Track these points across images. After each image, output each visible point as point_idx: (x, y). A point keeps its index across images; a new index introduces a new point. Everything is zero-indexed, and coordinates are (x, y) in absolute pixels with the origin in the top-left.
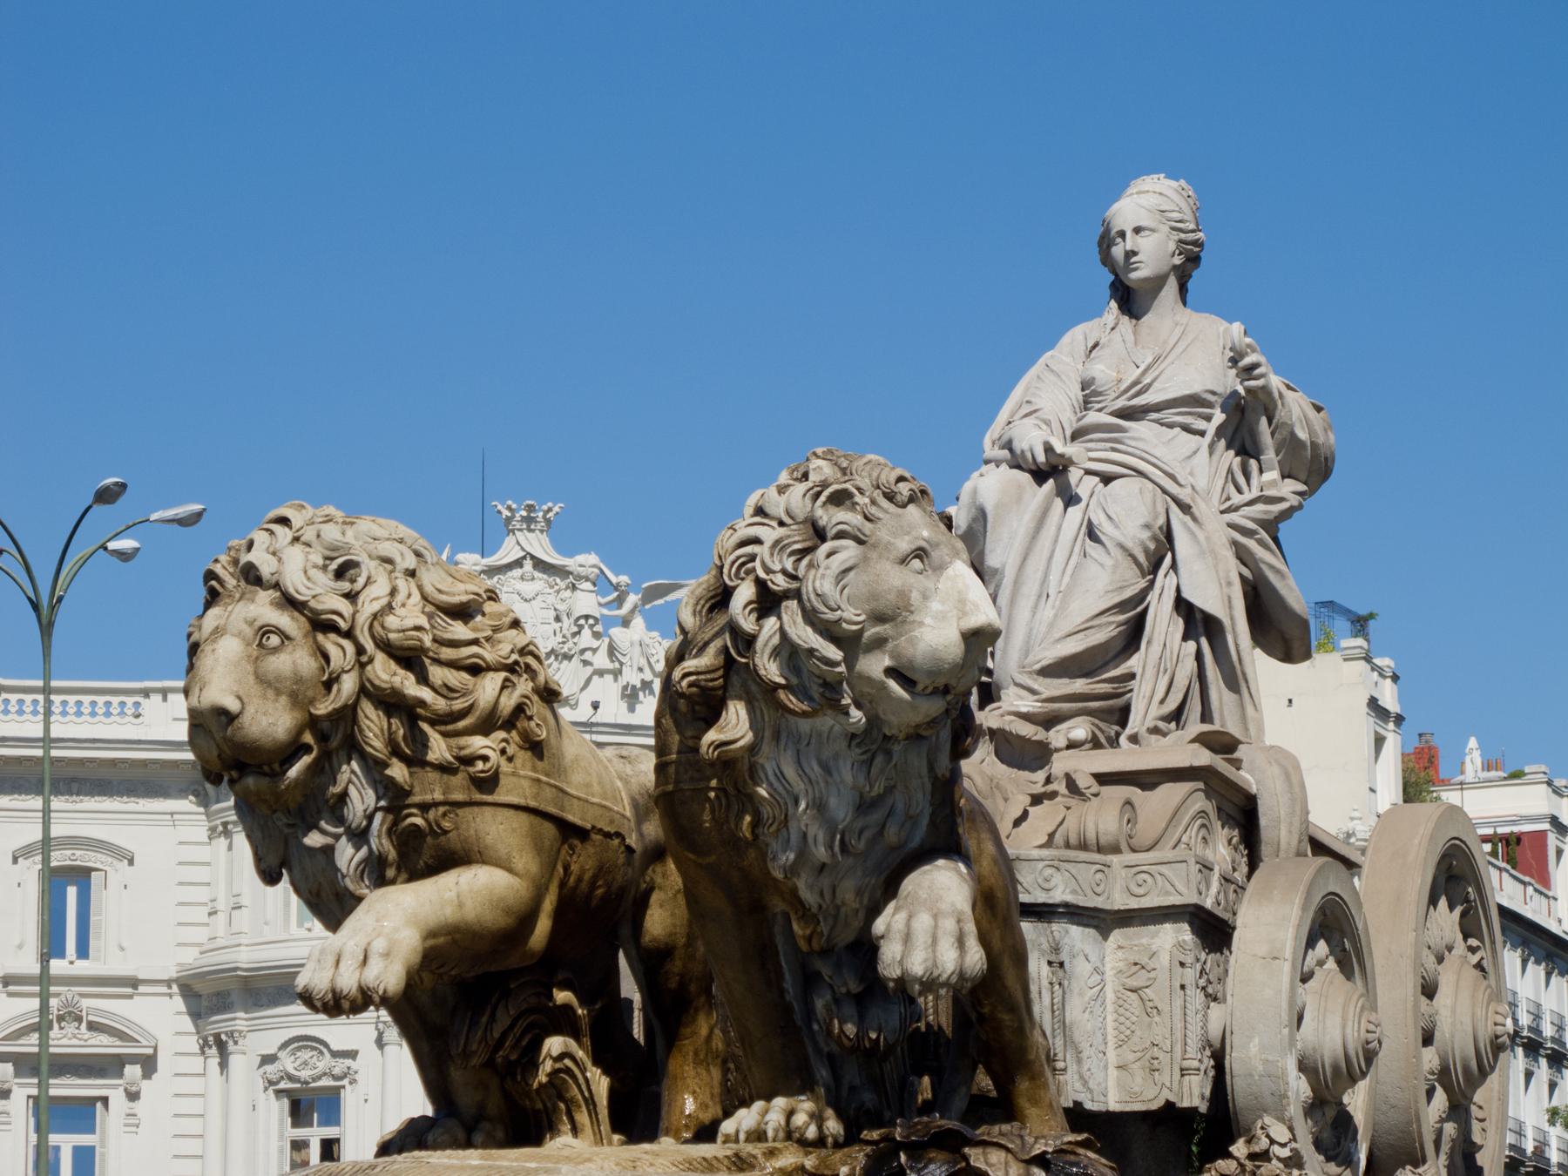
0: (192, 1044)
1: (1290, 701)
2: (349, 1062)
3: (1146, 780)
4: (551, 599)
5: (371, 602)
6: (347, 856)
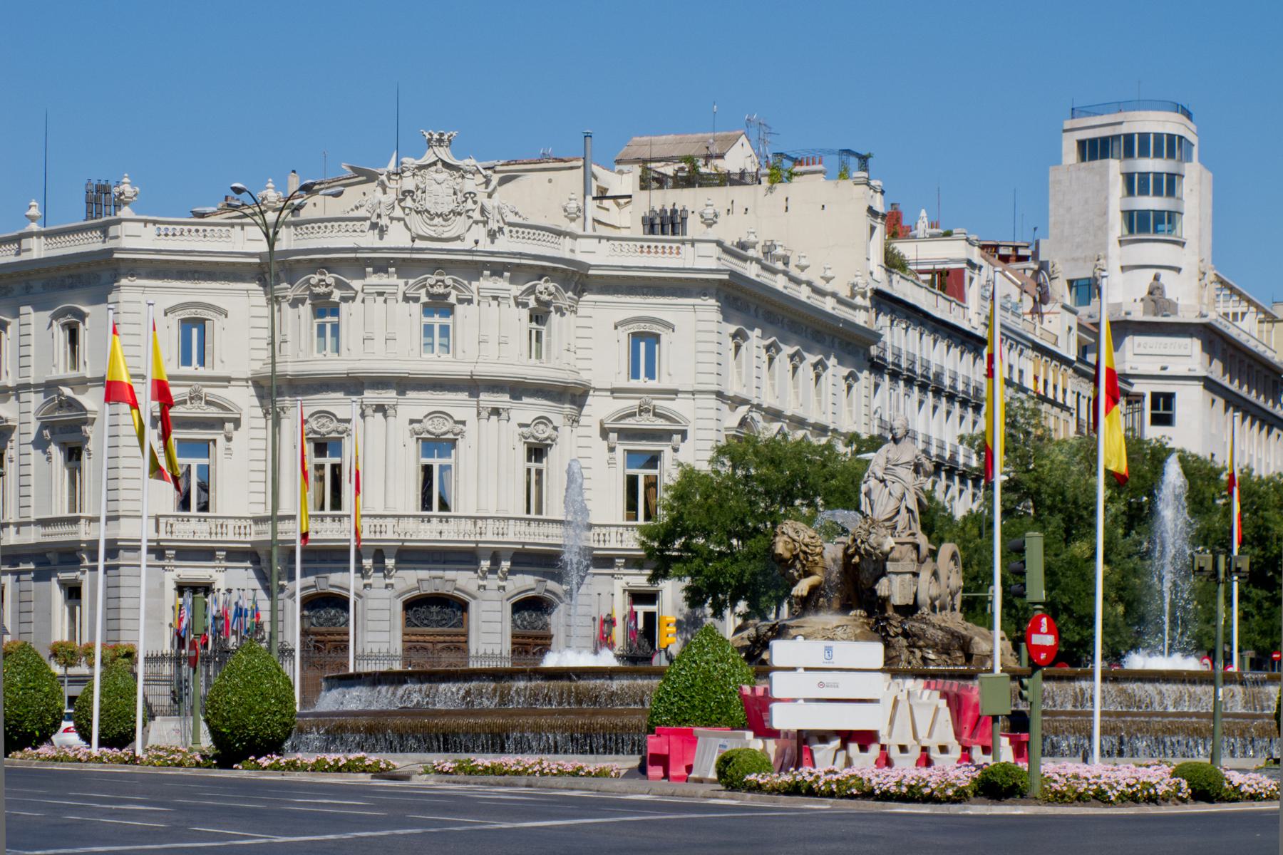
0: (259, 412)
2: (346, 425)
3: (902, 544)
4: (451, 183)
5: (801, 537)
6: (796, 574)
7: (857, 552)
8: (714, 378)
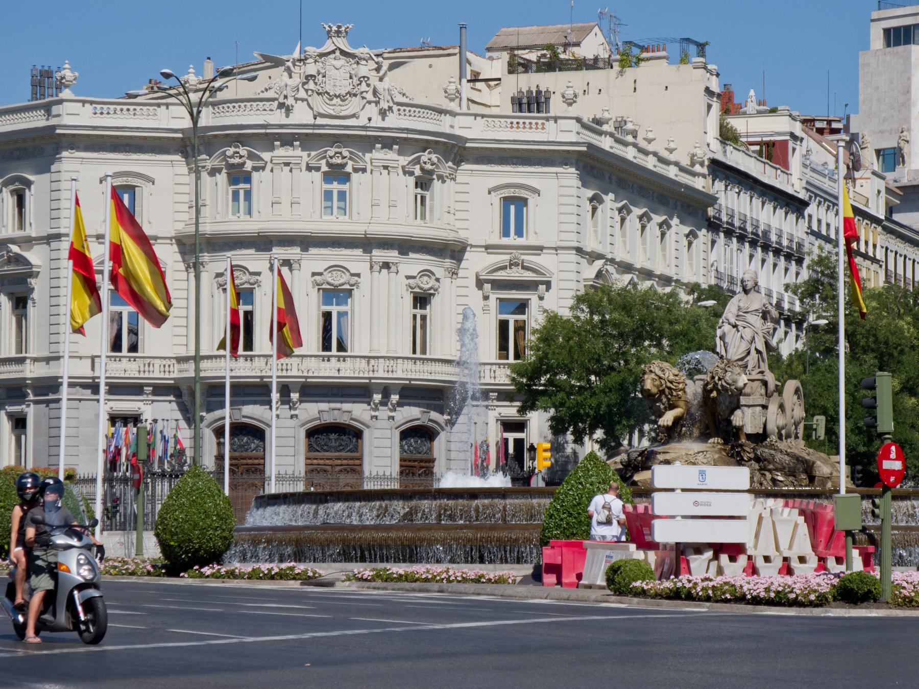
0: (182, 266)
1: (667, 87)
2: (257, 277)
3: (753, 380)
4: (348, 69)
6: (662, 407)
7: (715, 387)
8: (574, 236)
